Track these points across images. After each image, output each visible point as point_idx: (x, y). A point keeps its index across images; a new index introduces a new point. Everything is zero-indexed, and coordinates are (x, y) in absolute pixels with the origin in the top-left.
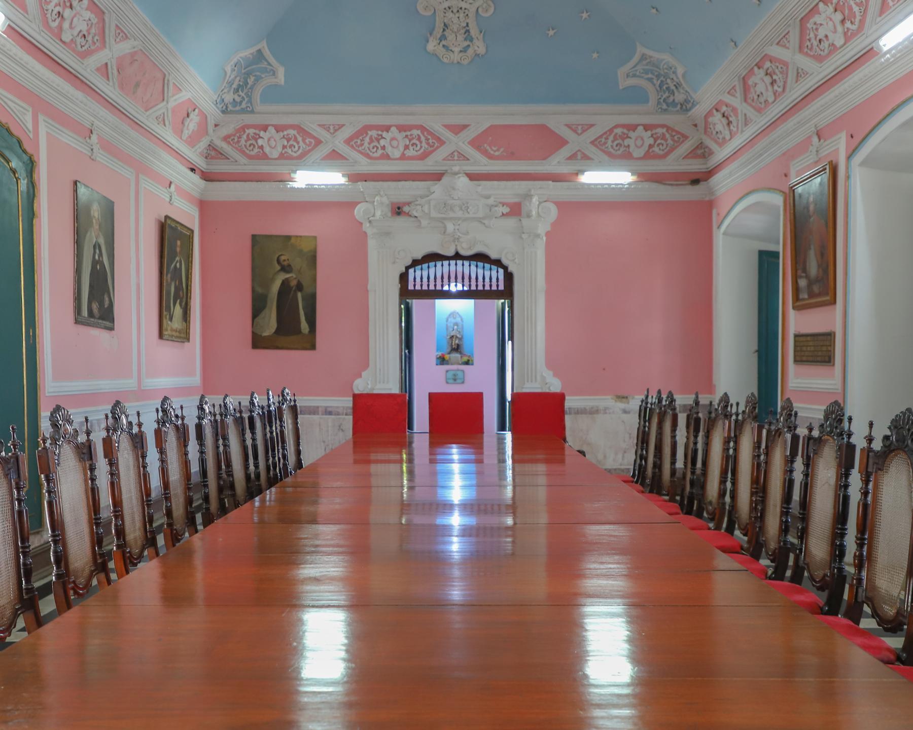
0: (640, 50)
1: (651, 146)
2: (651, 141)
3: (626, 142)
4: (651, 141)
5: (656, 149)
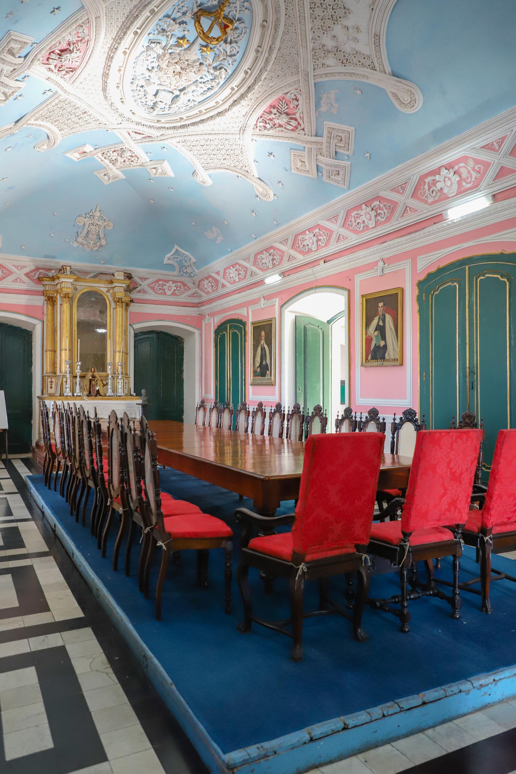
0: (176, 247)
1: (174, 290)
2: (175, 288)
3: (164, 287)
4: (175, 288)
5: (176, 292)
